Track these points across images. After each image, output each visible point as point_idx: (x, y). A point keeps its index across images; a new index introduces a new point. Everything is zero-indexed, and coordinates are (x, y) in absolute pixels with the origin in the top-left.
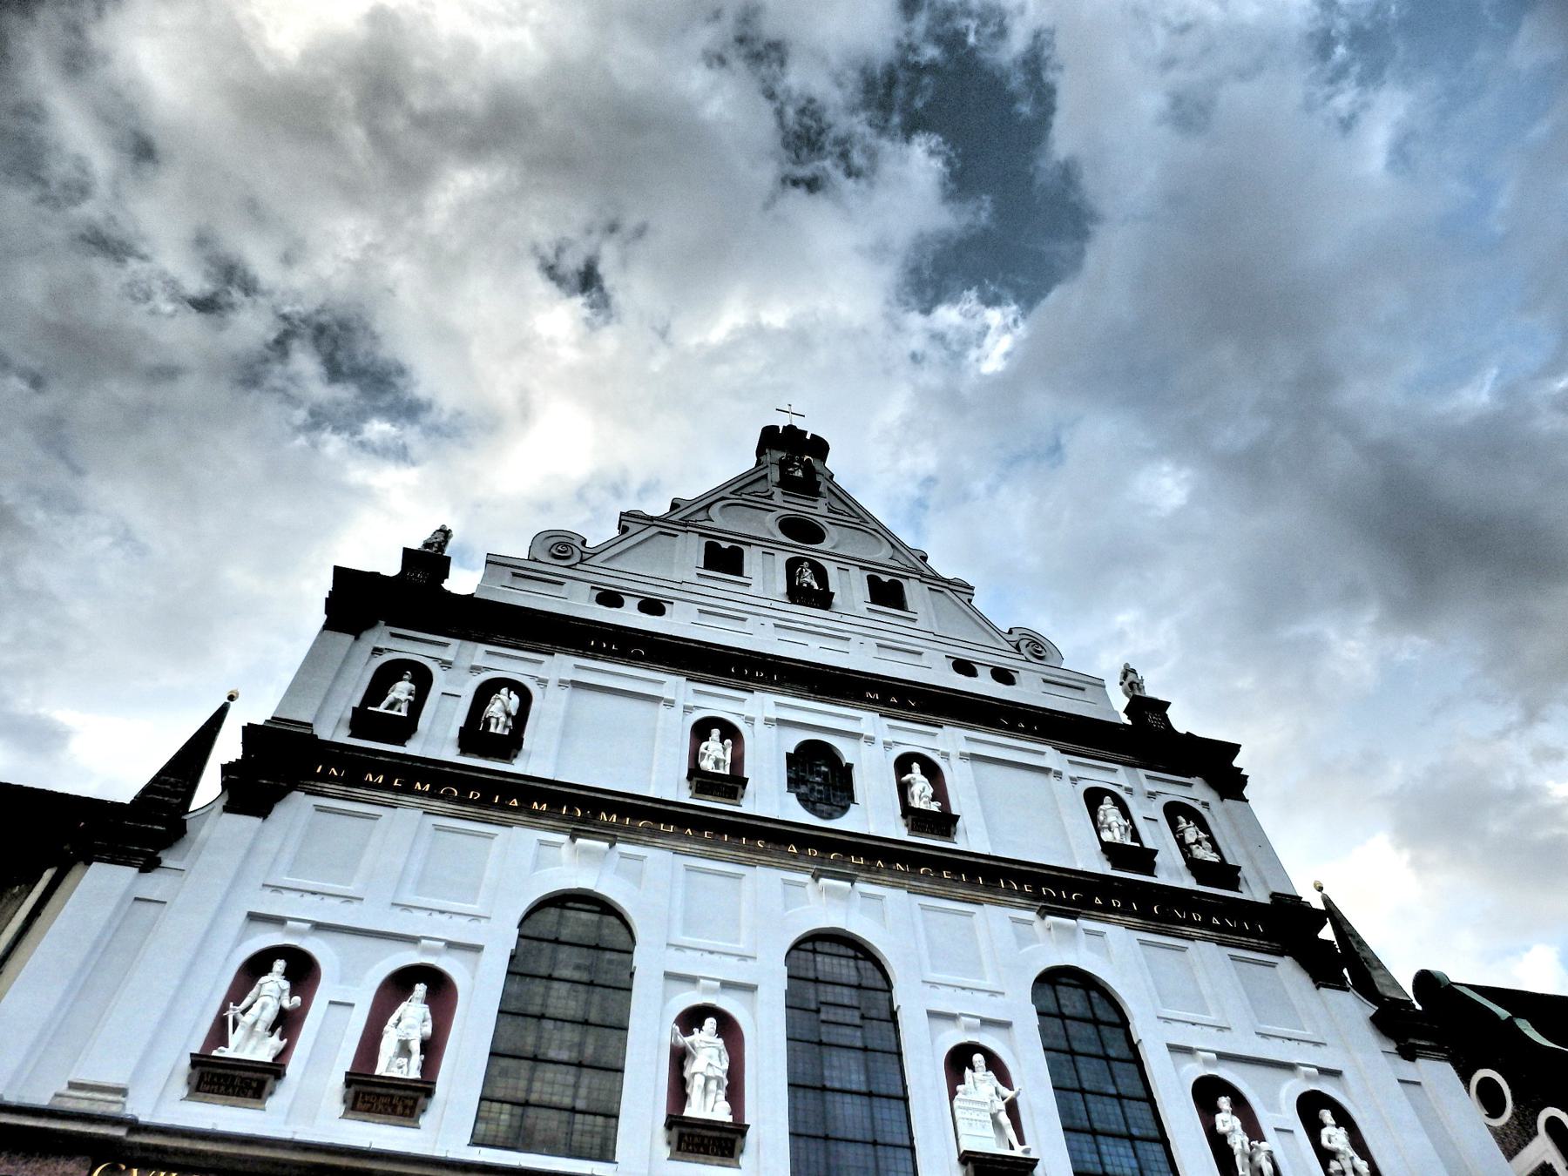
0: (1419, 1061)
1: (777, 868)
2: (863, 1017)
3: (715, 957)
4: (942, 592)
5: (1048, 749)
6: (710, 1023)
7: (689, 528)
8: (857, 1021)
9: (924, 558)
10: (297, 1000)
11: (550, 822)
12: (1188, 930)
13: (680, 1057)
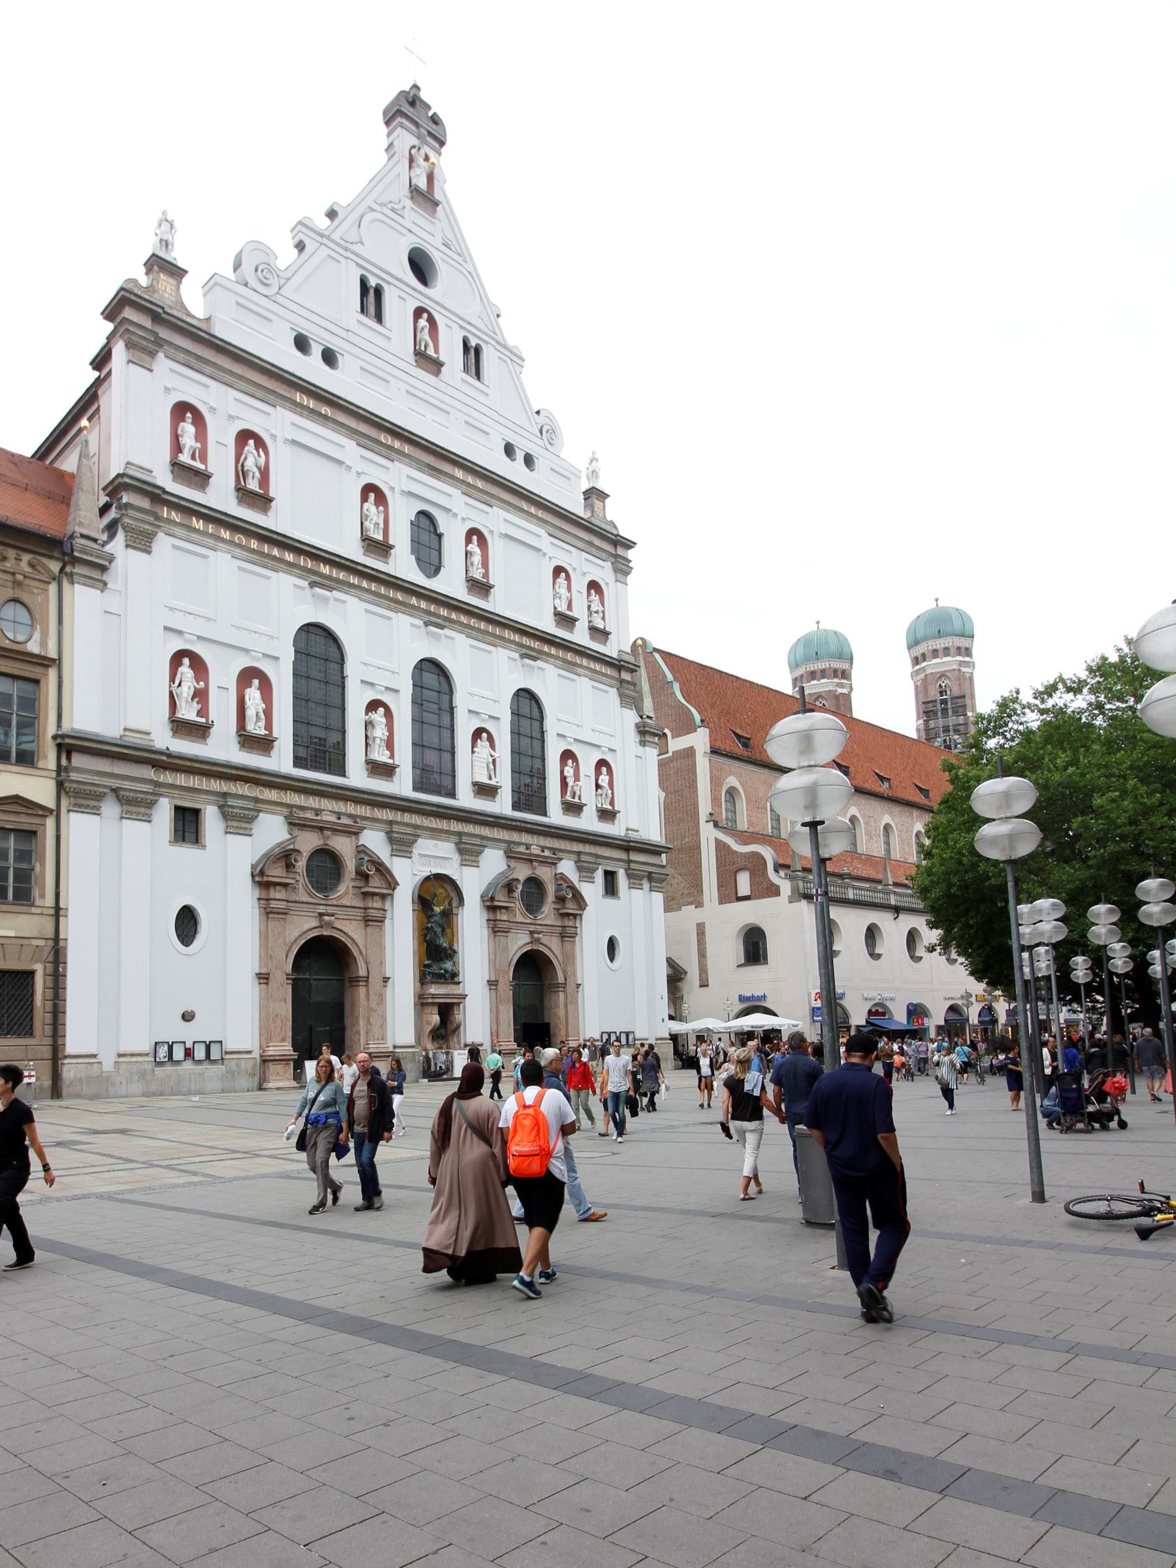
0: (647, 748)
1: (408, 615)
2: (440, 709)
3: (381, 671)
4: (505, 361)
5: (541, 532)
6: (381, 710)
7: (349, 255)
8: (437, 711)
9: (498, 316)
10: (202, 684)
11: (298, 571)
12: (580, 670)
13: (368, 724)
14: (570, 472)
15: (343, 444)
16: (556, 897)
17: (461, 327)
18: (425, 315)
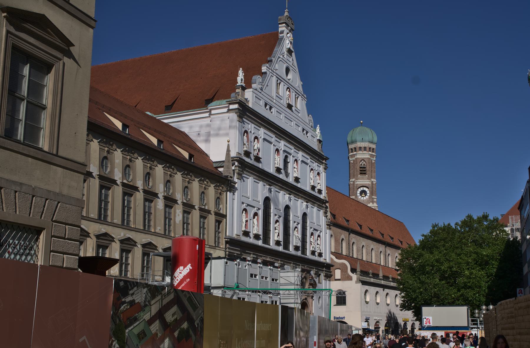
12: (316, 205)
14: (315, 135)
15: (272, 137)
16: (309, 283)
17: (296, 92)
18: (288, 90)
